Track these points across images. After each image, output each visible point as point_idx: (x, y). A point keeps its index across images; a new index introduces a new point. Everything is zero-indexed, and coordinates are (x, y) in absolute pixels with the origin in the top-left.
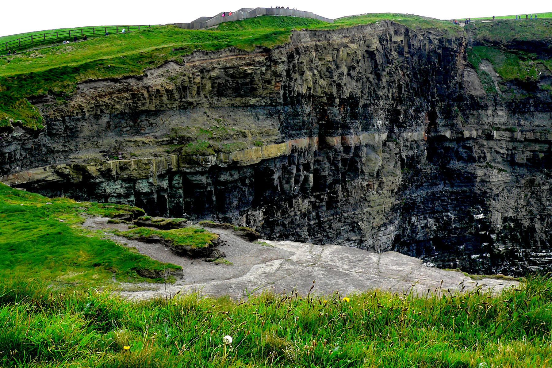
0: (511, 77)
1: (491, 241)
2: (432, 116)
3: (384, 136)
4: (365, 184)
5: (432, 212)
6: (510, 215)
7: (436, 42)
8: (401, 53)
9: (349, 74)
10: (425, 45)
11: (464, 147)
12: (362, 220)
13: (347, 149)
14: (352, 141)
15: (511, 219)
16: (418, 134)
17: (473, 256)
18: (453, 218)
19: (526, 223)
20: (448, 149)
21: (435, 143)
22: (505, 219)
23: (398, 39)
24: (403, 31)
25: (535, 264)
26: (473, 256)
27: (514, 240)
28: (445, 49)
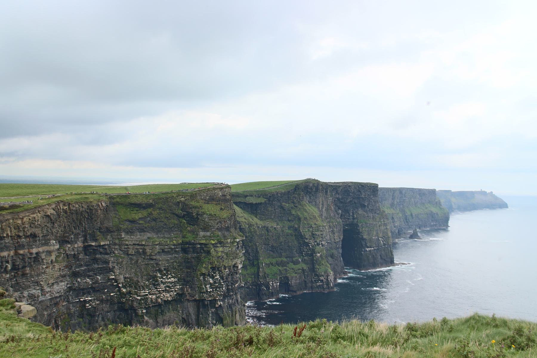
1: (119, 287)
2: (85, 236)
3: (57, 247)
4: (44, 266)
5: (89, 276)
6: (127, 276)
7: (86, 207)
9: (30, 226)
11: (103, 249)
12: (42, 281)
13: (31, 254)
14: (34, 251)
15: (128, 278)
17: (112, 294)
18: (100, 278)
19: (135, 279)
20: (94, 250)
21: (86, 248)
22: (125, 278)
23: (65, 208)
24: (67, 204)
25: (140, 296)
26: (112, 294)
27: (130, 286)
28: (90, 209)
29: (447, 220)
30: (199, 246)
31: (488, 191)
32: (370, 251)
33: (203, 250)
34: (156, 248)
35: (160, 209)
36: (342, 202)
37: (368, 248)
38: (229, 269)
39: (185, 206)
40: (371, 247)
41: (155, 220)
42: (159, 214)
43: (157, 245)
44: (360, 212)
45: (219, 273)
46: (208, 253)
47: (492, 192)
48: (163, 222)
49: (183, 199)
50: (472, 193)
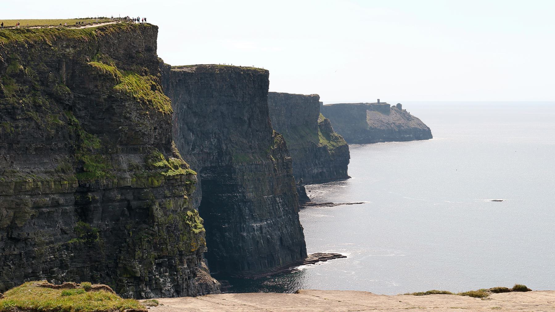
29: (345, 159)
30: (119, 197)
31: (393, 103)
32: (261, 228)
33: (129, 208)
34: (26, 205)
36: (195, 114)
37: (256, 221)
38: (190, 262)
39: (80, 75)
40: (261, 221)
43: (26, 192)
45: (171, 275)
46: (146, 215)
47: (399, 106)
48: (31, 119)
49: (71, 50)
50: (362, 108)
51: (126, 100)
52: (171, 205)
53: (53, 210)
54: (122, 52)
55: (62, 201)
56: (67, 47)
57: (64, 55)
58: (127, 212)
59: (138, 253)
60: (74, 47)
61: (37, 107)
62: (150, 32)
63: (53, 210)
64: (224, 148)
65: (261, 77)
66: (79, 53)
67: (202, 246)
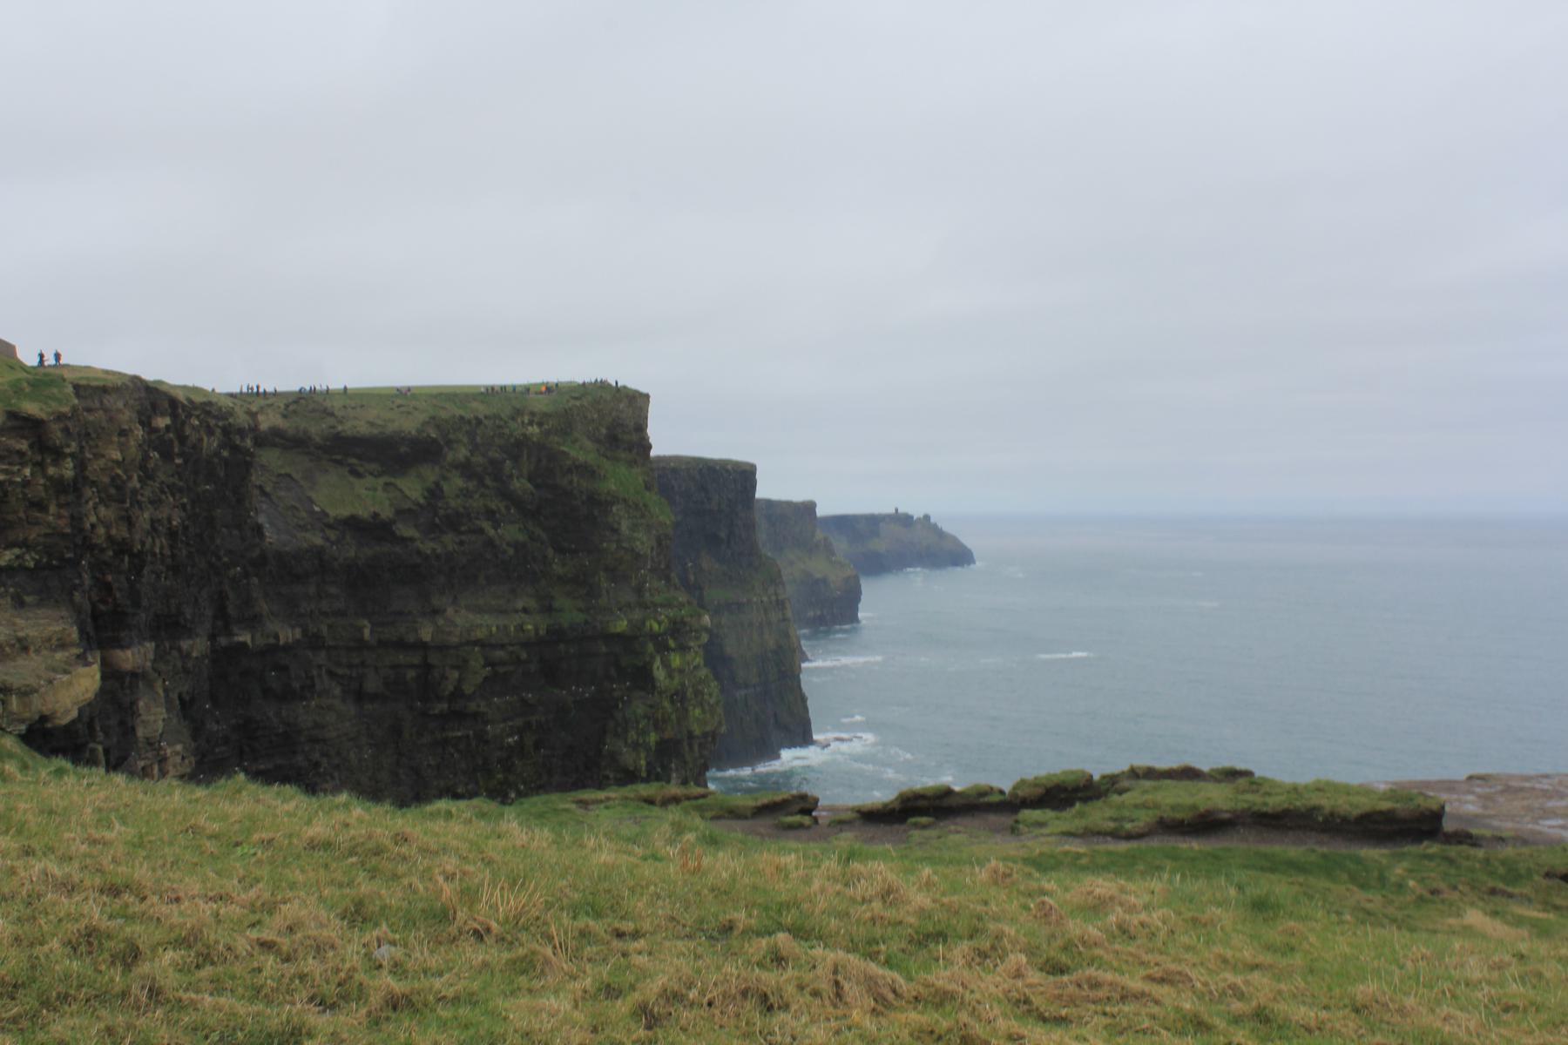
0: (345, 512)
7: (218, 431)
8: (167, 456)
10: (201, 440)
16: (197, 646)
28: (235, 449)
30: (604, 649)
31: (917, 512)
35: (465, 468)
41: (453, 522)
42: (466, 494)
44: (707, 563)
46: (643, 678)
47: (927, 517)
48: (481, 531)
50: (873, 521)
51: (612, 504)
52: (676, 660)
53: (511, 668)
54: (604, 431)
55: (524, 656)
56: (531, 423)
57: (524, 435)
58: (613, 672)
59: (632, 735)
60: (540, 424)
61: (490, 514)
62: (637, 402)
63: (511, 668)
64: (692, 578)
65: (745, 476)
66: (548, 433)
67: (720, 723)
